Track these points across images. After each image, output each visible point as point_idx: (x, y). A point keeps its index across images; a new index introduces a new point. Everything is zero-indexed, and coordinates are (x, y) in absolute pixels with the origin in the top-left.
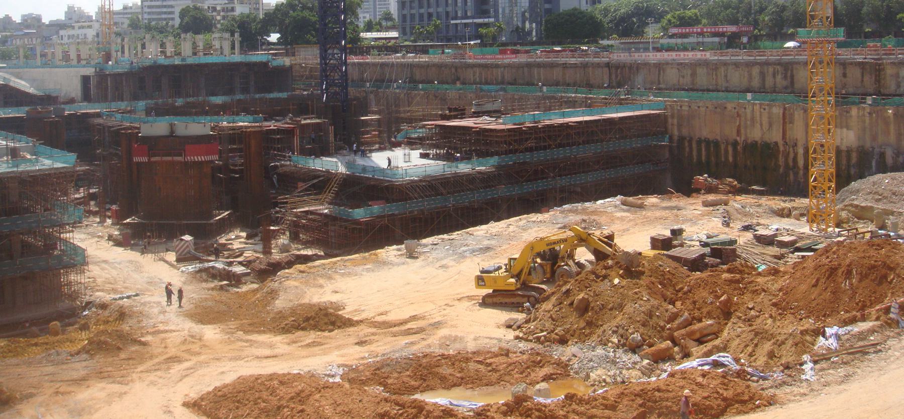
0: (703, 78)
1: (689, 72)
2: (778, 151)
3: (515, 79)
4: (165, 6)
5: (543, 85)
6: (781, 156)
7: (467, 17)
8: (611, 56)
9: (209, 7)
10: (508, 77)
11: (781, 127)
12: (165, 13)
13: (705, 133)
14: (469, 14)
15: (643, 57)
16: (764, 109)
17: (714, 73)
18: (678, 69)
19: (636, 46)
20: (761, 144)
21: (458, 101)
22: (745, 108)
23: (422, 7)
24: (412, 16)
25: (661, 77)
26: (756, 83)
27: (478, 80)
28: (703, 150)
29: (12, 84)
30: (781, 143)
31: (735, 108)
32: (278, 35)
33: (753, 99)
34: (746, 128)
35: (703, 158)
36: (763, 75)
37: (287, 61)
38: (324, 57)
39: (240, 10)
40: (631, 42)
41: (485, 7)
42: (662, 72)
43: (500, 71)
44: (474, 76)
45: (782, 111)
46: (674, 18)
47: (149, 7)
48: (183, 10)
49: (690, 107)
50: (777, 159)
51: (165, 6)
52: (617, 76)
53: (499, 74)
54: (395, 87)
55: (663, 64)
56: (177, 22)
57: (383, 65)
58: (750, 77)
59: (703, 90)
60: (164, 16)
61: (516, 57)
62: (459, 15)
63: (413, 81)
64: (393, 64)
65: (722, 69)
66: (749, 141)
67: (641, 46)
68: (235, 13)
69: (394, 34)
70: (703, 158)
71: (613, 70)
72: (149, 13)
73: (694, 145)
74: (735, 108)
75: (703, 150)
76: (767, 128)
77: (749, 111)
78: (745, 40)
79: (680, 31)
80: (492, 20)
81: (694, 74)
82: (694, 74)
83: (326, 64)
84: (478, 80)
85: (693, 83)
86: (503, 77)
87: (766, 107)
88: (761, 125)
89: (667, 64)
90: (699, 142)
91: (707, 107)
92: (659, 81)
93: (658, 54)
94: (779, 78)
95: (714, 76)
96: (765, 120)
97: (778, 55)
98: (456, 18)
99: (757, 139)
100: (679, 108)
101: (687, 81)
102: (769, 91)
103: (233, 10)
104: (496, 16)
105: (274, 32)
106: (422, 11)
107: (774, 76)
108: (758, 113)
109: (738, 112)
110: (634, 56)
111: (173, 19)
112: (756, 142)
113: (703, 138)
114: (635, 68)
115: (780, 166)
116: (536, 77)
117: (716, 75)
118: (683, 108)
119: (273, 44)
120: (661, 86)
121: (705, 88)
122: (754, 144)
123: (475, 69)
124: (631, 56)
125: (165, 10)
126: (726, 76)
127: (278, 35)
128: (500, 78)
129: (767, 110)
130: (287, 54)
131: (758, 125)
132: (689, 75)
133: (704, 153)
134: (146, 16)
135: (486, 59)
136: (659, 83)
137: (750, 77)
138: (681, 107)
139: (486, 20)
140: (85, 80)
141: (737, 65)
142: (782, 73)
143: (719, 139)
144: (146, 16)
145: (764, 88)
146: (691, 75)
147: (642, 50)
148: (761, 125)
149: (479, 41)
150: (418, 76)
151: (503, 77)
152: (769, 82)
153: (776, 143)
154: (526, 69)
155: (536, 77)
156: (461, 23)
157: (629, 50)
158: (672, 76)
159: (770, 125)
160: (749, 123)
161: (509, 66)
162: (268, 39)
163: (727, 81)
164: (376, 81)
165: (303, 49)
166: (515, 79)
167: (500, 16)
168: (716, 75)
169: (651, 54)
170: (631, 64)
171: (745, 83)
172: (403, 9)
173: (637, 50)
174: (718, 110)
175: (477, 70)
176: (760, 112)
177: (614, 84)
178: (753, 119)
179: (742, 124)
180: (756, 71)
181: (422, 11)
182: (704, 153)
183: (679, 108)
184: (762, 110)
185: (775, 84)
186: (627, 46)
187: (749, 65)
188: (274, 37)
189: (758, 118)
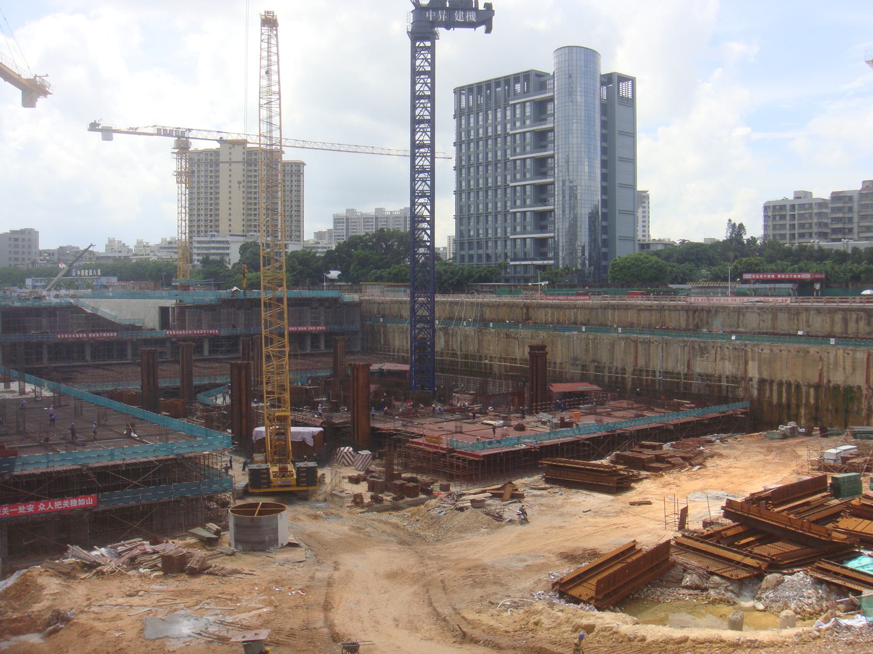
0: (783, 324)
1: (770, 316)
2: (862, 395)
3: (589, 320)
4: (214, 242)
5: (618, 327)
6: (864, 398)
8: (688, 300)
10: (581, 318)
11: (865, 370)
12: (214, 248)
13: (785, 376)
15: (722, 301)
16: (848, 354)
17: (796, 318)
18: (759, 313)
19: (715, 290)
20: (844, 387)
21: (530, 340)
22: (828, 353)
23: (472, 249)
24: (471, 257)
25: (740, 321)
26: (838, 329)
27: (550, 320)
28: (784, 392)
29: (99, 314)
30: (864, 386)
31: (818, 353)
32: (339, 272)
33: (836, 344)
34: (828, 372)
35: (784, 400)
36: (845, 321)
37: (355, 297)
38: (413, 297)
39: (292, 248)
40: (705, 287)
41: (544, 250)
42: (741, 317)
43: (572, 312)
44: (546, 315)
45: (865, 356)
46: (741, 264)
47: (199, 242)
49: (771, 350)
50: (860, 402)
51: (214, 242)
52: (694, 319)
53: (572, 313)
54: (465, 324)
55: (743, 308)
56: (234, 256)
57: (452, 304)
58: (833, 322)
59: (785, 335)
60: (212, 251)
61: (589, 299)
63: (483, 322)
64: (462, 303)
65: (803, 316)
66: (831, 385)
67: (719, 290)
68: (287, 250)
70: (784, 400)
71: (691, 313)
72: (198, 248)
73: (775, 387)
74: (818, 353)
75: (784, 392)
76: (851, 372)
77: (832, 356)
78: (817, 286)
79: (754, 276)
80: (552, 262)
81: (775, 319)
82: (775, 319)
83: (415, 302)
84: (550, 320)
85: (773, 328)
86: (576, 317)
87: (850, 352)
88: (844, 369)
89: (747, 308)
90: (780, 384)
91: (789, 351)
92: (738, 324)
93: (738, 299)
94: (862, 324)
95: (795, 321)
96: (848, 364)
97: (861, 302)
98: (515, 260)
99: (839, 383)
100: (760, 351)
101: (767, 326)
102: (851, 336)
103: (286, 246)
104: (556, 257)
105: (335, 269)
106: (480, 252)
107: (857, 322)
108: (841, 358)
109: (820, 357)
110: (713, 300)
111: (228, 254)
112: (839, 386)
113: (784, 381)
114: (711, 311)
115: (862, 409)
116: (610, 319)
117: (798, 320)
118: (765, 351)
119: (333, 280)
120: (740, 329)
121: (786, 332)
122: (837, 388)
123: (547, 309)
124: (709, 300)
125: (213, 245)
126: (808, 321)
127: (339, 272)
128: (572, 318)
129: (851, 355)
130: (351, 290)
131: (841, 369)
132: (769, 320)
133: (784, 395)
134: (195, 251)
135: (558, 299)
136: (738, 327)
137: (833, 322)
138: (762, 350)
139: (546, 262)
140: (164, 311)
141: (818, 311)
142: (865, 320)
143: (801, 383)
144: (195, 251)
145: (847, 333)
146: (772, 319)
147: (720, 295)
148: (844, 369)
149: (547, 283)
150: (488, 314)
151: (576, 317)
152: (852, 328)
153: (859, 388)
154: (600, 311)
155: (610, 319)
156: (520, 265)
157: (707, 294)
158: (752, 321)
159: (854, 369)
160: (831, 367)
161: (582, 307)
162: (328, 276)
163: (809, 326)
164: (445, 319)
165: (370, 287)
166: (589, 320)
168: (798, 320)
169: (730, 299)
170: (709, 307)
171: (827, 328)
172: (462, 249)
173: (716, 294)
174: (801, 353)
175: (550, 311)
176: (844, 357)
177: (691, 327)
178: (836, 363)
179: (825, 369)
180: (838, 317)
181: (480, 252)
182: (784, 395)
183: (760, 351)
184: (846, 355)
185: (858, 330)
186: (703, 290)
187: (832, 311)
188: (334, 274)
189: (841, 363)
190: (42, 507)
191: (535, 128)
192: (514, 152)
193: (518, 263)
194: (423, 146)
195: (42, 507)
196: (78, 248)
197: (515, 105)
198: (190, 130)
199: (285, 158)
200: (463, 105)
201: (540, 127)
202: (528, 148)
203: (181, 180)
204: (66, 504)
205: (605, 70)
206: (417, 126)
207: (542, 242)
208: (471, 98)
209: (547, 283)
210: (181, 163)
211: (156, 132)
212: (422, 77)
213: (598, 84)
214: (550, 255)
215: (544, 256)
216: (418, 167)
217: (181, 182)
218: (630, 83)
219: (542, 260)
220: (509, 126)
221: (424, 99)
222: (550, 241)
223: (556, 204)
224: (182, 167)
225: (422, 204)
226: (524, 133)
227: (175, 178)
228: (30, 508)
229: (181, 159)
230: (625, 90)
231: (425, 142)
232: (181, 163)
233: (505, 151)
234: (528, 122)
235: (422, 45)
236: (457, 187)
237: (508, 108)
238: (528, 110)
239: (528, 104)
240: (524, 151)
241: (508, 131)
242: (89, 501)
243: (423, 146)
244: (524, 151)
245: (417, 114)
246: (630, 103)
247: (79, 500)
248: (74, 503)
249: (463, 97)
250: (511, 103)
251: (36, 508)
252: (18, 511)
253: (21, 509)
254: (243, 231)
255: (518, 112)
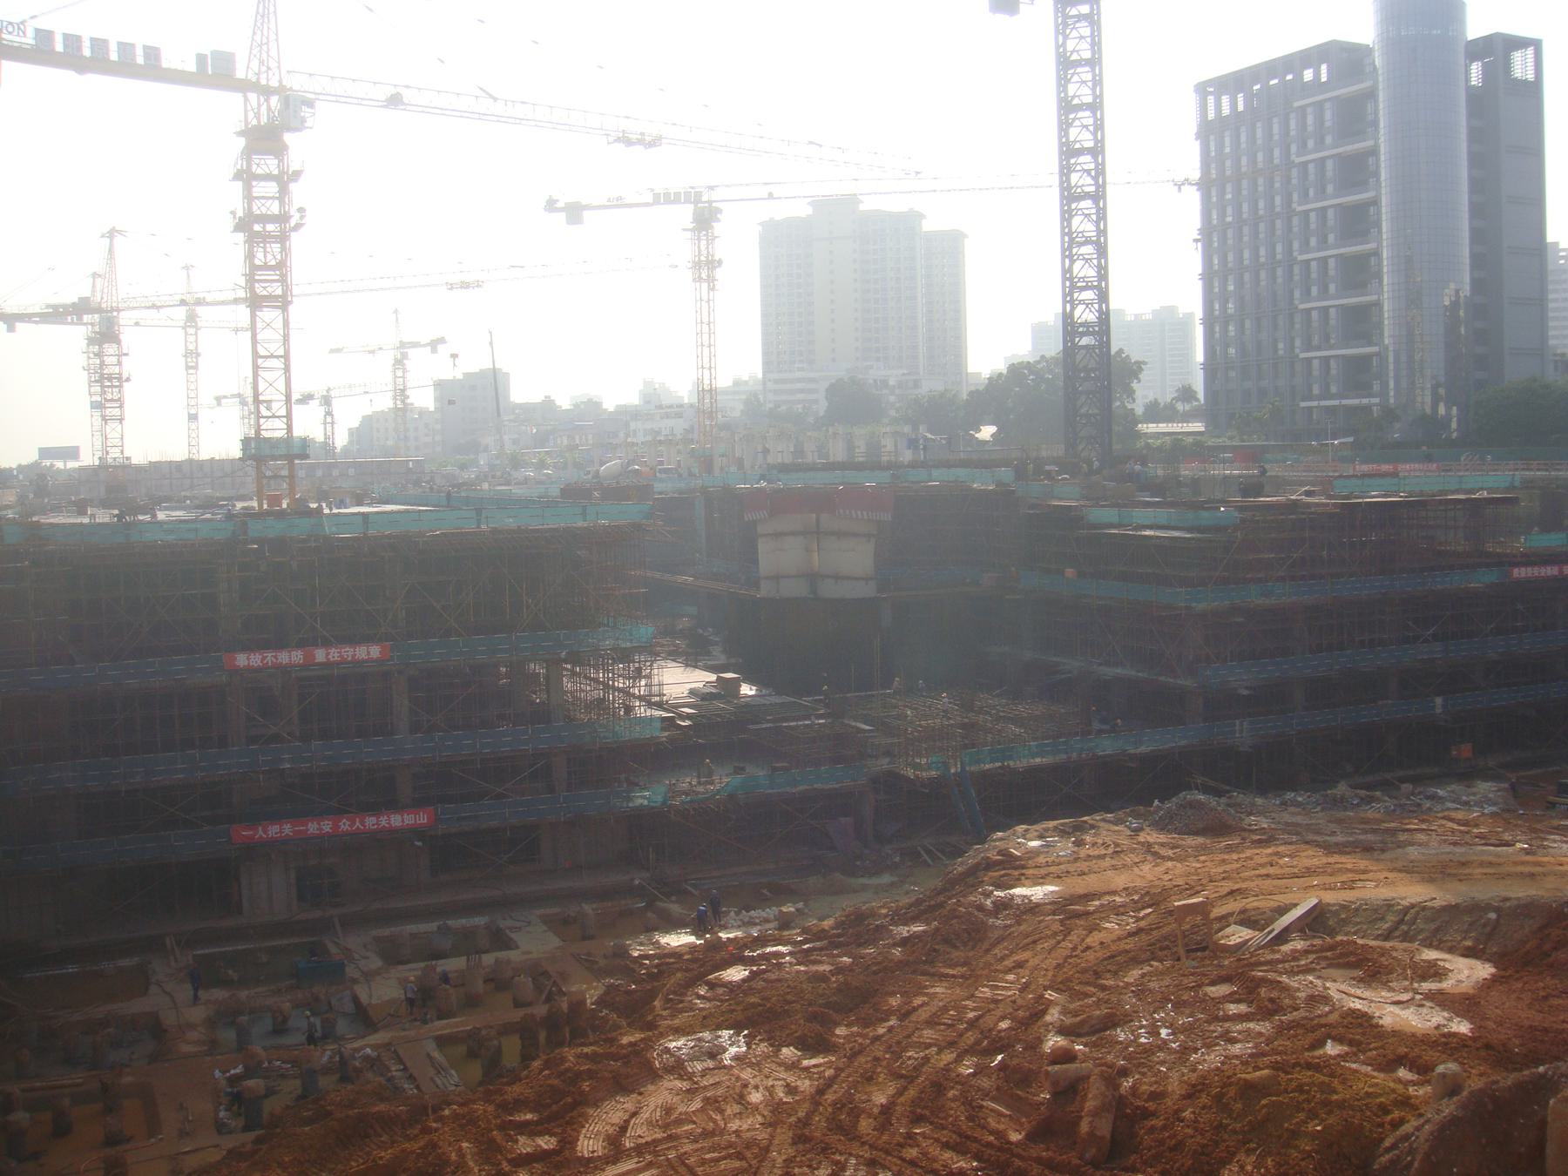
7: (1332, 397)
9: (875, 381)
14: (1334, 389)
32: (992, 429)
47: (776, 382)
48: (832, 385)
62: (1316, 390)
69: (1198, 427)
80: (1376, 400)
98: (1310, 398)
111: (816, 401)
127: (992, 429)
139: (1365, 401)
149: (1351, 439)
162: (977, 435)
167: (1392, 393)
190: (344, 825)
191: (1340, 150)
192: (1305, 197)
193: (1315, 403)
194: (1086, 196)
195: (344, 825)
196: (548, 403)
197: (1303, 109)
198: (711, 188)
199: (928, 226)
200: (1211, 115)
201: (1349, 148)
202: (1330, 189)
203: (699, 276)
204: (384, 821)
205: (1476, 27)
206: (1073, 161)
207: (1362, 363)
208: (1225, 100)
209: (1351, 439)
210: (699, 247)
211: (651, 201)
212: (1079, 70)
213: (1462, 61)
214: (1376, 387)
215: (1362, 388)
216: (1075, 235)
217: (700, 279)
218: (1530, 51)
219: (1358, 397)
220: (1294, 148)
221: (1084, 110)
222: (1375, 361)
223: (1387, 294)
224: (700, 254)
225: (1082, 302)
226: (1323, 160)
227: (689, 275)
228: (327, 826)
229: (699, 239)
230: (1522, 65)
231: (1087, 189)
232: (699, 247)
233: (1290, 195)
234: (1329, 140)
235: (1074, 12)
236: (1204, 270)
237: (1293, 116)
238: (1328, 115)
239: (1328, 105)
240: (1322, 193)
241: (1293, 157)
242: (423, 819)
243: (1086, 196)
244: (1322, 193)
245: (1072, 139)
246: (1532, 91)
247: (405, 816)
248: (396, 820)
249: (1211, 100)
250: (1296, 104)
251: (336, 827)
252: (308, 830)
253: (312, 828)
254: (857, 359)
255: (1310, 120)
